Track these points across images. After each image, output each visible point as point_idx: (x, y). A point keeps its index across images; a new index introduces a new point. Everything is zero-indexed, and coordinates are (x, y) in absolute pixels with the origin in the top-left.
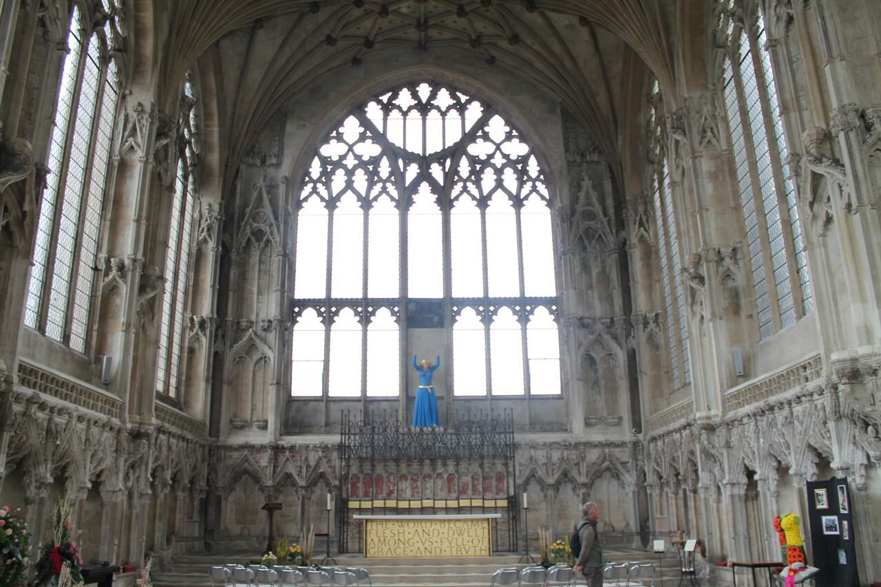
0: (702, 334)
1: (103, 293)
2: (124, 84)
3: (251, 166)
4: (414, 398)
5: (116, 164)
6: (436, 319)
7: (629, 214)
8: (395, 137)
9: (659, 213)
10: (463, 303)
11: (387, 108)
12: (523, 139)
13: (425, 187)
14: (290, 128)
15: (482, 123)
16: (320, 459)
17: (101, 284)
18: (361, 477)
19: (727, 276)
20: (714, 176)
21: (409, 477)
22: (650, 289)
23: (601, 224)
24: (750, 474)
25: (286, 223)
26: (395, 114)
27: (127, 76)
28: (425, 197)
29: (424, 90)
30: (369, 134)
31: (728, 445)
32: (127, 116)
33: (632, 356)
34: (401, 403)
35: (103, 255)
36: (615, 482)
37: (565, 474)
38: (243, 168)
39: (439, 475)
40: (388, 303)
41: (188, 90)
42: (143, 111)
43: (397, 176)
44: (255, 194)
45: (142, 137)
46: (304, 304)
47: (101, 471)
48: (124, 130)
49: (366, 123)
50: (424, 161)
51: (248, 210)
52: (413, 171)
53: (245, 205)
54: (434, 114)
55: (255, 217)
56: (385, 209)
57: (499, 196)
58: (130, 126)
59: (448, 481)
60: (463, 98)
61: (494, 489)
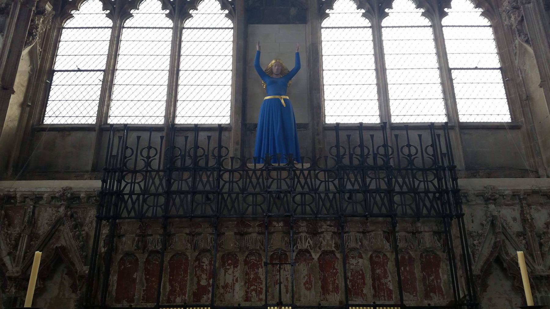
4: (256, 126)
6: (293, 11)
16: (59, 222)
18: (142, 258)
21: (241, 258)
34: (232, 134)
39: (304, 254)
59: (321, 266)
61: (419, 286)
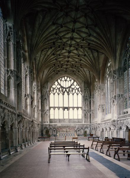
0: (99, 113)
3: (44, 89)
7: (91, 96)
8: (62, 85)
9: (95, 97)
10: (70, 107)
11: (61, 80)
12: (78, 85)
14: (49, 83)
15: (73, 83)
19: (103, 107)
20: (103, 95)
22: (93, 106)
23: (88, 98)
24: (103, 129)
26: (62, 81)
28: (66, 93)
29: (66, 78)
31: (101, 126)
33: (90, 114)
36: (87, 129)
37: (82, 128)
40: (62, 107)
43: (62, 90)
44: (44, 93)
46: (51, 107)
47: (5, 122)
49: (58, 83)
50: (66, 88)
52: (64, 90)
54: (67, 81)
55: (45, 96)
56: (61, 95)
57: (75, 93)
60: (71, 79)
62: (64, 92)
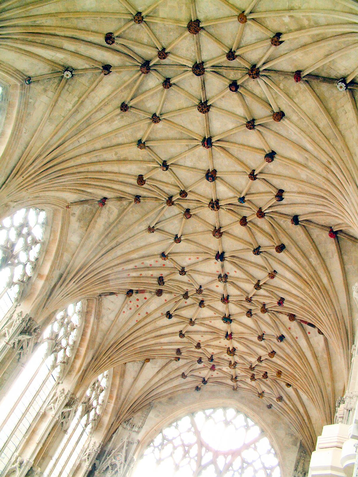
1: (9, 472)
2: (61, 378)
5: (41, 414)
11: (208, 417)
13: (212, 467)
14: (152, 415)
17: (9, 468)
25: (129, 465)
27: (63, 375)
30: (193, 429)
32: (55, 393)
35: (17, 454)
38: (120, 428)
41: (104, 383)
42: (63, 393)
43: (200, 457)
44: (121, 444)
45: (58, 405)
48: (51, 399)
49: (193, 424)
50: (216, 454)
51: (113, 451)
52: (207, 457)
53: (113, 449)
58: (55, 398)
62: (205, 467)
